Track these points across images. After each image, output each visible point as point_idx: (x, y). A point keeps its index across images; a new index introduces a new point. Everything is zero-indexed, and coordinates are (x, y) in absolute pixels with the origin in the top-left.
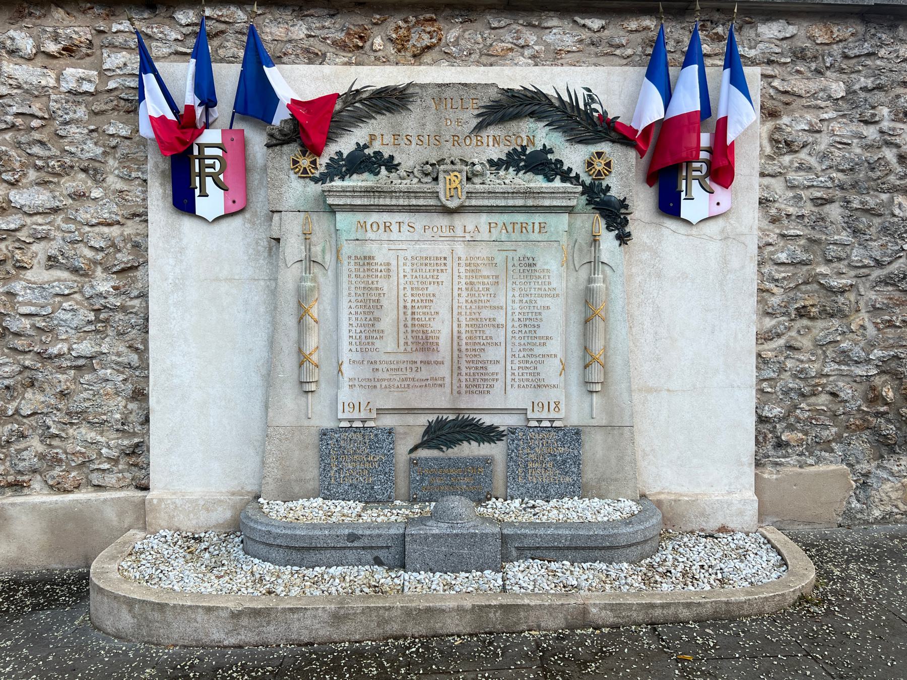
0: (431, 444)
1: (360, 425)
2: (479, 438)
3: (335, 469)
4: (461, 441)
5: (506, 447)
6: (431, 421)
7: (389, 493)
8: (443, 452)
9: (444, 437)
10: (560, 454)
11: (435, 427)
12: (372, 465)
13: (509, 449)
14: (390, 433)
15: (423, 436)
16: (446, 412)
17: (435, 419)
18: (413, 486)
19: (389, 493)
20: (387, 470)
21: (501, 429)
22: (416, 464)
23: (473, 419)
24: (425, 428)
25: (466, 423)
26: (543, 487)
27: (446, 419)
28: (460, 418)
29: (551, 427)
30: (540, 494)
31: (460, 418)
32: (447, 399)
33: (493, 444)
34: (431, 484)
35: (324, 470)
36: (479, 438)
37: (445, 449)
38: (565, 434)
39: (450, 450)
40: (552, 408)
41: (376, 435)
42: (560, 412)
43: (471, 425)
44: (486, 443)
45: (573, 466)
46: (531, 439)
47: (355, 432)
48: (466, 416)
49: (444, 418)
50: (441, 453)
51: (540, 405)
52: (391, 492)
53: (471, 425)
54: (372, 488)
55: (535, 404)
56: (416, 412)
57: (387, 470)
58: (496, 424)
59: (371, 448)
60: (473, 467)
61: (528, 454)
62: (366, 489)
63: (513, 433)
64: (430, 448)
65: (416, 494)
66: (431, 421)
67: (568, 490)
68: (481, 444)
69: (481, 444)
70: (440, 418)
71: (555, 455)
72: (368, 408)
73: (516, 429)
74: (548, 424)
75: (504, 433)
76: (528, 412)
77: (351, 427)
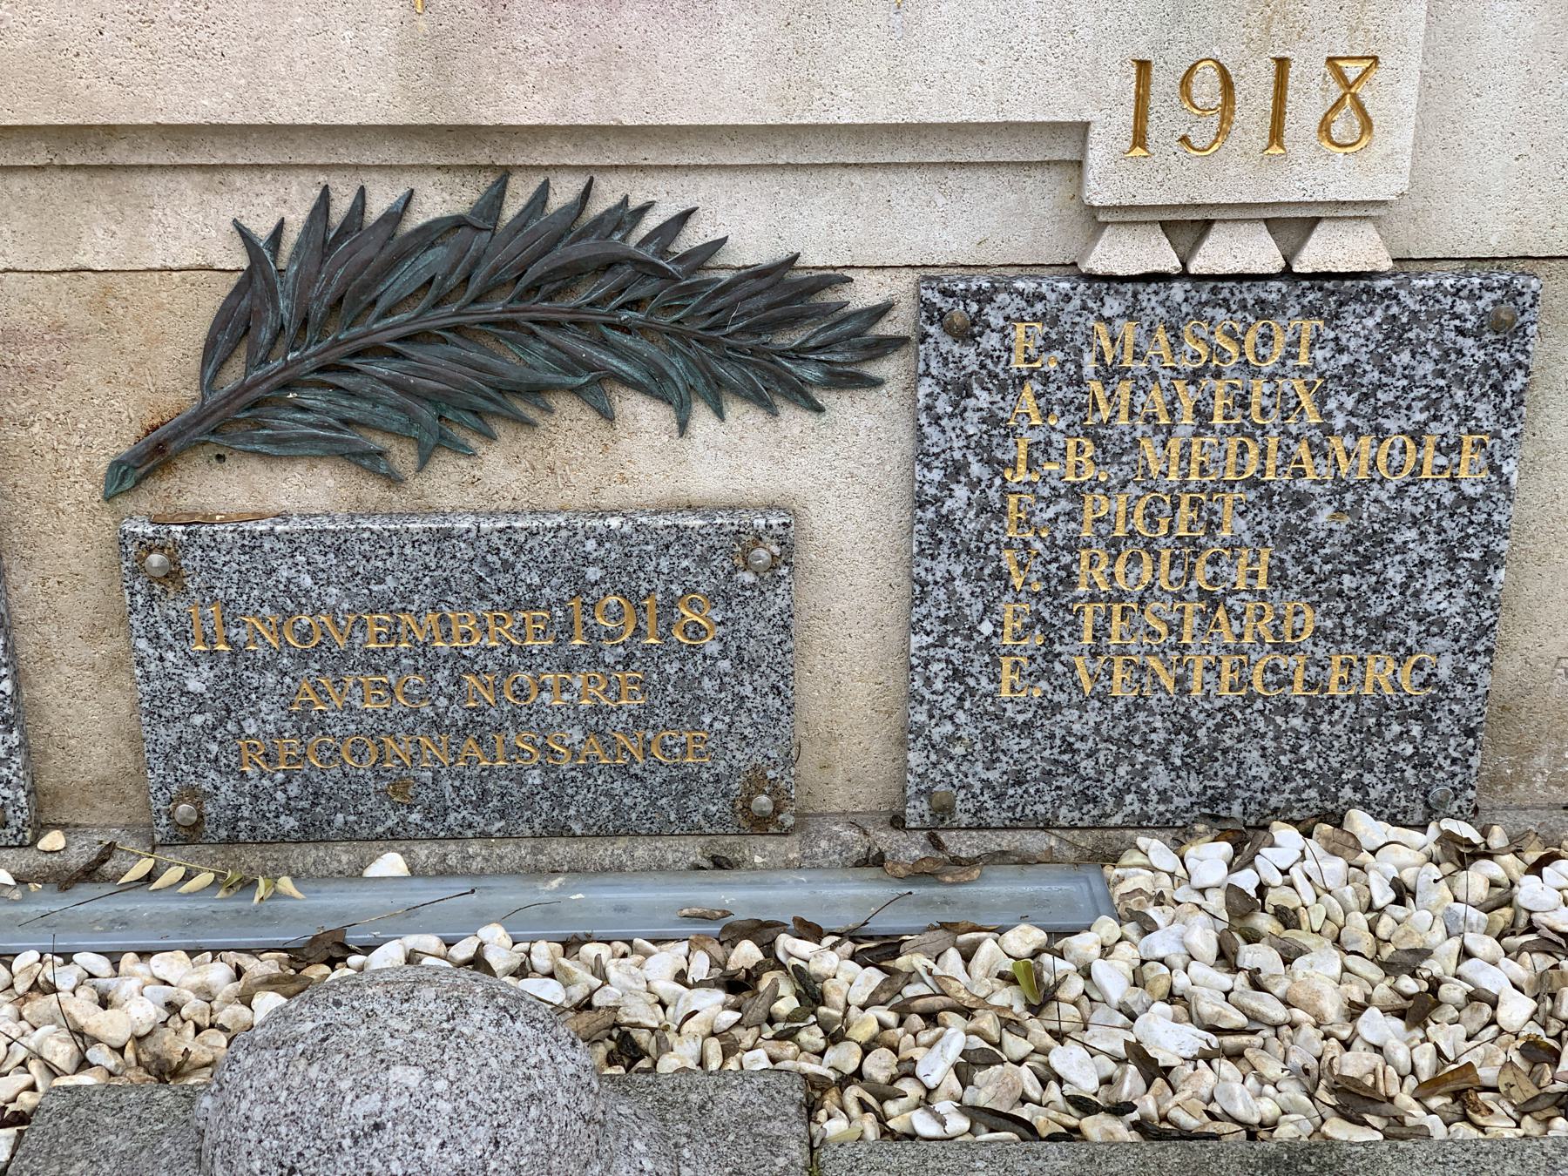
0: (287, 423)
2: (676, 367)
4: (536, 391)
5: (903, 433)
6: (262, 229)
8: (393, 480)
9: (383, 369)
10: (1342, 487)
11: (305, 282)
13: (923, 457)
15: (215, 353)
16: (387, 153)
17: (297, 220)
18: (168, 736)
21: (864, 293)
22: (173, 575)
24: (224, 287)
26: (1183, 726)
27: (395, 216)
28: (511, 209)
29: (1287, 274)
30: (1161, 777)
31: (511, 209)
32: (380, 40)
33: (793, 419)
36: (676, 367)
37: (402, 456)
38: (1395, 333)
40: (1304, 110)
42: (1380, 143)
43: (608, 265)
44: (736, 410)
45: (1434, 577)
46: (1110, 373)
48: (564, 193)
49: (378, 206)
50: (373, 491)
51: (1206, 88)
55: (1164, 82)
56: (118, 153)
58: (814, 257)
60: (631, 595)
61: (1075, 492)
63: (965, 334)
64: (281, 450)
65: (192, 794)
66: (262, 229)
67: (1376, 753)
68: (702, 417)
69: (702, 417)
70: (341, 206)
71: (1300, 500)
73: (985, 298)
74: (1261, 253)
75: (886, 328)
76: (1097, 155)
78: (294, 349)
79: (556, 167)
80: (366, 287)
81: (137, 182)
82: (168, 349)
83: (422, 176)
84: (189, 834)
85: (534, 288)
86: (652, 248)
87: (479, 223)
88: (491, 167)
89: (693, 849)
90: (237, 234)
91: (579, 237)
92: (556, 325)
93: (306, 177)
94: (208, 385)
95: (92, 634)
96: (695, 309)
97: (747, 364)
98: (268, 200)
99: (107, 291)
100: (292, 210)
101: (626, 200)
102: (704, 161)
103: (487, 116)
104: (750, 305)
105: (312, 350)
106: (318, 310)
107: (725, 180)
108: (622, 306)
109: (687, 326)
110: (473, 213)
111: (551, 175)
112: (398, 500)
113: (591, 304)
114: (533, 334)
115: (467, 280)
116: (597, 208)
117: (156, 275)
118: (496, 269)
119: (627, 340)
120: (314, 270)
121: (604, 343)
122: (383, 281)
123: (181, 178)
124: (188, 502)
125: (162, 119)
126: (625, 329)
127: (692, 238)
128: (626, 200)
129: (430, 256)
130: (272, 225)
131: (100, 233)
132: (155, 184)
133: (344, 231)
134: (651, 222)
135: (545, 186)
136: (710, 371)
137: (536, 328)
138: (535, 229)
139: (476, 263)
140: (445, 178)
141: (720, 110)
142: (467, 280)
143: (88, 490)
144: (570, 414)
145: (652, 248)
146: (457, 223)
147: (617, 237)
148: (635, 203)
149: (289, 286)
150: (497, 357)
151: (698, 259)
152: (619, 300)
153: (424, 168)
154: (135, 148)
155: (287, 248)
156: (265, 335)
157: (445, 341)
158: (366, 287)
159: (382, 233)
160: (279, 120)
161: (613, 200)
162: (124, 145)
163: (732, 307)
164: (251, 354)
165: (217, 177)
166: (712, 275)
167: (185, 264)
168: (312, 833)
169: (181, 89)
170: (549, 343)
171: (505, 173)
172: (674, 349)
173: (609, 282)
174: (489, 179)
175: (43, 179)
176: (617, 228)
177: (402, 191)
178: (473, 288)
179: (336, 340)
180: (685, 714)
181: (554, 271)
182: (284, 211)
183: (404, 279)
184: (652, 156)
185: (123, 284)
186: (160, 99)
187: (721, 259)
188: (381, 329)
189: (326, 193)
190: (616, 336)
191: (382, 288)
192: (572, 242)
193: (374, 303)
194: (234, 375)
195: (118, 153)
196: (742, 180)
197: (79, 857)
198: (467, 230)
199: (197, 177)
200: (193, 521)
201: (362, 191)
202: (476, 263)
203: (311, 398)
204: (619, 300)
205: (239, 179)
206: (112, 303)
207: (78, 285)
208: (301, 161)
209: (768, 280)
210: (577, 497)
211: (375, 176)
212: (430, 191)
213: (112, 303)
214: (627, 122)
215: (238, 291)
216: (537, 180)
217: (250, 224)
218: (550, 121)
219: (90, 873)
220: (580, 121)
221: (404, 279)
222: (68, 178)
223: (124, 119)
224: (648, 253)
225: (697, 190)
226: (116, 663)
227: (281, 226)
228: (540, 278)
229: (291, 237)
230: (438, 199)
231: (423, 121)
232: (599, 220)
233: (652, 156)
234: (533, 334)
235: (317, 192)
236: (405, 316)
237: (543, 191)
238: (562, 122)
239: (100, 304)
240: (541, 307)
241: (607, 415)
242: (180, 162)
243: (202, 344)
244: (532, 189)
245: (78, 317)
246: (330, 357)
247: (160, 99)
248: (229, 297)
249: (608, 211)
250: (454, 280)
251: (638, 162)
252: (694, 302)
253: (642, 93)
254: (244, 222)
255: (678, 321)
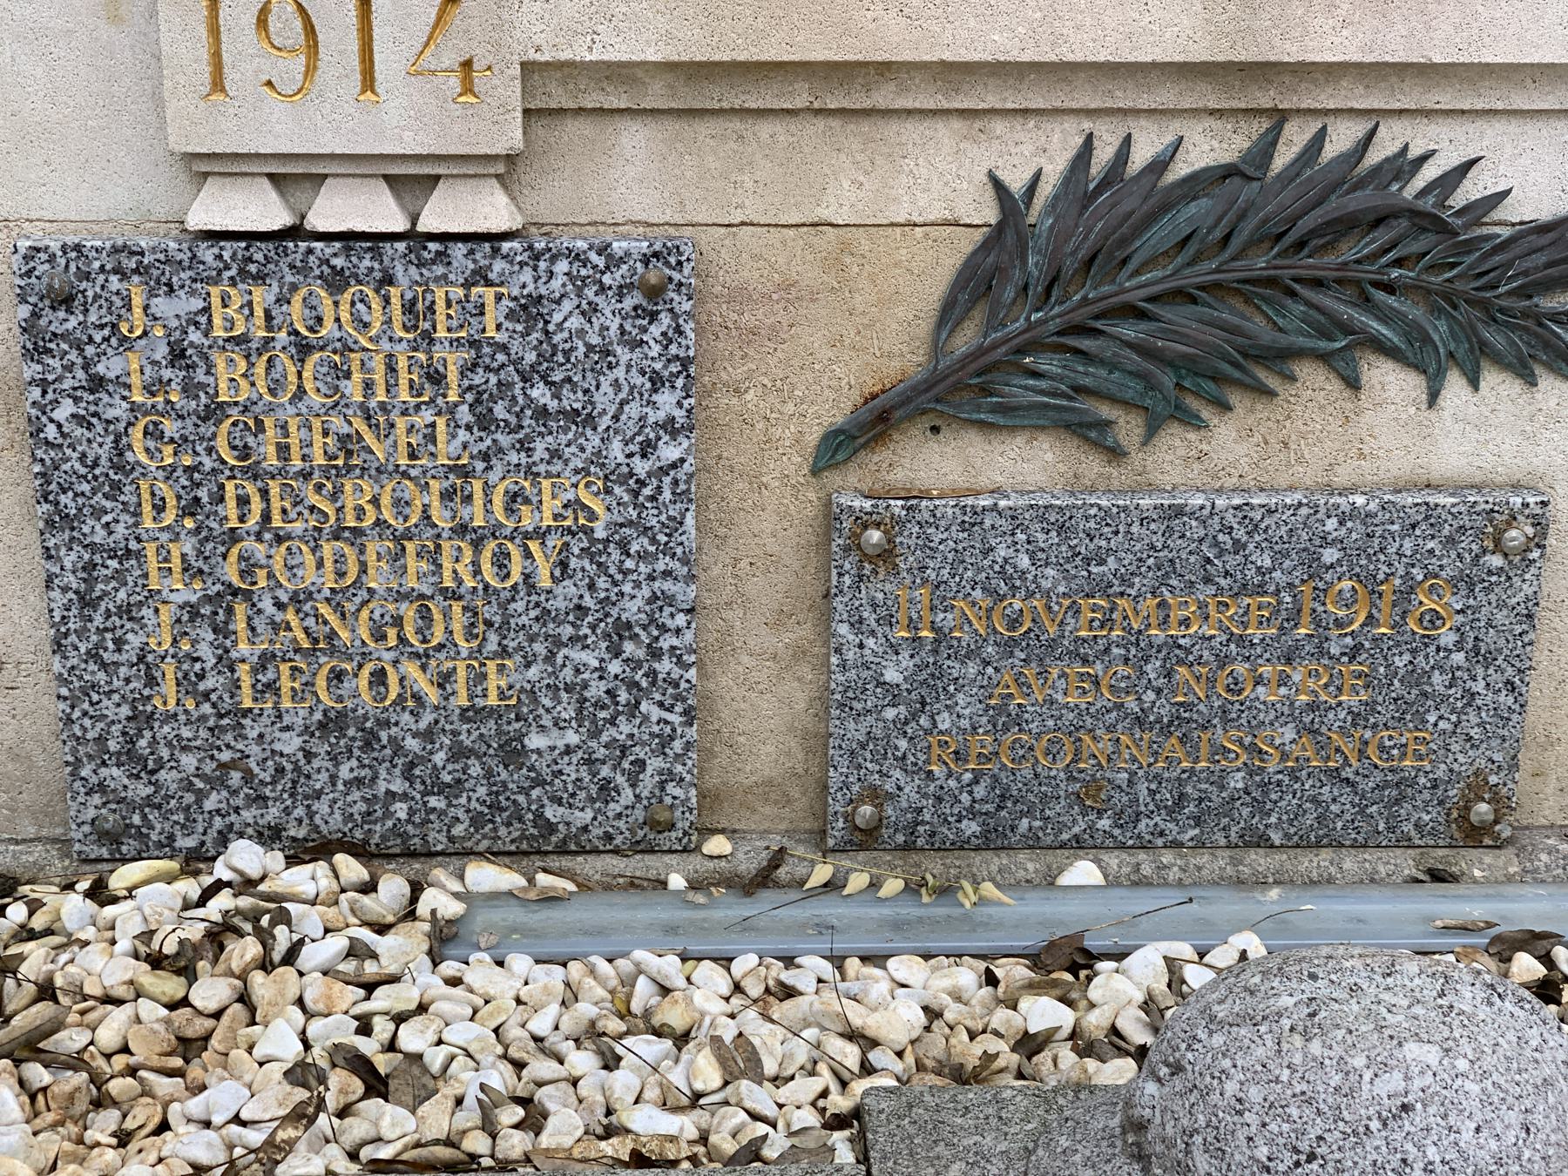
0: (1019, 390)
1: (384, 214)
2: (1439, 330)
3: (183, 592)
4: (1280, 358)
6: (1016, 182)
7: (648, 782)
8: (1115, 453)
9: (1129, 331)
11: (1059, 236)
12: (501, 561)
14: (654, 292)
15: (950, 313)
17: (1055, 169)
18: (856, 731)
19: (648, 782)
20: (632, 609)
22: (886, 555)
23: (1404, 166)
24: (967, 242)
25: (1336, 206)
27: (1159, 165)
28: (1283, 158)
31: (1283, 158)
34: (1004, 718)
35: (87, 602)
36: (1439, 330)
37: (1128, 427)
39: (1175, 444)
41: (529, 310)
44: (1492, 378)
47: (336, 282)
48: (1342, 137)
49: (1141, 156)
50: (1093, 466)
52: (666, 777)
53: (1378, 222)
54: (513, 752)
56: (884, 97)
57: (632, 609)
59: (485, 422)
62: (459, 753)
65: (875, 795)
68: (1455, 385)
69: (1455, 385)
70: (1103, 155)
72: (451, 59)
77: (295, 232)
78: (1037, 310)
79: (1337, 112)
80: (1124, 242)
81: (892, 128)
82: (900, 312)
83: (1192, 123)
84: (864, 839)
85: (1300, 245)
86: (1431, 200)
87: (1250, 171)
88: (1276, 110)
89: (1406, 863)
90: (989, 186)
91: (1355, 188)
92: (1318, 283)
93: (1070, 124)
94: (937, 347)
95: (779, 621)
96: (1470, 267)
97: (1514, 328)
98: (1027, 149)
99: (845, 248)
100: (1051, 160)
101: (1406, 148)
102: (1500, 106)
103: (1290, 52)
104: (1528, 263)
105: (1057, 310)
106: (1070, 265)
107: (1513, 127)
108: (1398, 263)
109: (1458, 285)
110: (1243, 159)
111: (1330, 120)
112: (1119, 475)
113: (1358, 262)
114: (1293, 294)
115: (1227, 238)
116: (1374, 157)
117: (898, 230)
118: (1265, 221)
119: (1391, 301)
120: (1071, 223)
121: (1366, 302)
122: (1140, 235)
123: (940, 125)
124: (899, 476)
125: (948, 56)
126: (1389, 288)
127: (1471, 190)
128: (1406, 148)
129: (1193, 209)
130: (1027, 175)
131: (846, 185)
132: (912, 131)
133: (1105, 183)
134: (1429, 172)
135: (1322, 133)
136: (1477, 335)
137: (1297, 287)
138: (1310, 179)
139: (1242, 216)
140: (1216, 124)
141: (1537, 47)
142: (1227, 238)
143: (796, 463)
144: (1314, 381)
145: (1431, 200)
146: (1227, 172)
147: (1395, 187)
148: (1414, 152)
149: (1042, 241)
150: (1244, 317)
151: (1480, 212)
152: (1391, 256)
153: (1195, 112)
154: (903, 90)
155: (1039, 202)
156: (1009, 293)
157: (1194, 300)
158: (1124, 242)
159: (1146, 182)
160: (1070, 58)
161: (1392, 149)
162: (892, 86)
163: (1509, 265)
164: (993, 314)
165: (978, 124)
166: (1485, 231)
167: (931, 218)
168: (993, 840)
169: (972, 23)
170: (1308, 304)
171: (1281, 117)
172: (1441, 310)
173: (1382, 236)
174: (1261, 126)
175: (794, 125)
176: (1396, 178)
177: (1169, 138)
178: (1236, 243)
179: (1085, 298)
180: (1410, 712)
181: (1328, 223)
182: (1042, 161)
183: (1163, 233)
184: (1444, 98)
185: (861, 238)
186: (948, 33)
187: (1497, 214)
188: (1134, 286)
189: (1089, 141)
190: (1380, 295)
191: (1138, 243)
192: (1348, 192)
193: (1124, 262)
194: (966, 339)
195: (884, 97)
196: (1531, 128)
197: (749, 862)
198: (1237, 180)
199: (957, 124)
200: (914, 497)
201: (1128, 140)
202: (1242, 216)
203: (1049, 364)
204: (1391, 256)
205: (999, 126)
206: (848, 260)
207: (816, 240)
208: (1074, 105)
209: (1551, 236)
210: (1309, 474)
211: (1143, 122)
212: (1197, 138)
213: (848, 260)
214: (1438, 59)
215: (985, 247)
216: (1314, 126)
217: (1004, 176)
218: (1357, 58)
219: (764, 879)
220: (1388, 59)
221: (1163, 233)
222: (821, 123)
223: (908, 56)
224: (1429, 203)
225: (1481, 137)
226: (799, 653)
227: (1037, 177)
228: (1311, 232)
229: (1046, 189)
230: (1206, 147)
231: (1221, 58)
232: (1377, 170)
233: (1446, 100)
234: (1293, 294)
235: (1079, 140)
236: (1160, 274)
237: (1320, 138)
238: (1369, 58)
239: (835, 262)
240: (1309, 264)
241: (1353, 384)
242: (946, 106)
243: (937, 305)
244: (1308, 136)
245: (811, 275)
246: (1077, 317)
247: (948, 33)
248: (974, 253)
249: (1387, 160)
250: (1218, 234)
251: (1430, 106)
252: (1469, 260)
253: (1457, 28)
254: (999, 174)
255: (1448, 280)
